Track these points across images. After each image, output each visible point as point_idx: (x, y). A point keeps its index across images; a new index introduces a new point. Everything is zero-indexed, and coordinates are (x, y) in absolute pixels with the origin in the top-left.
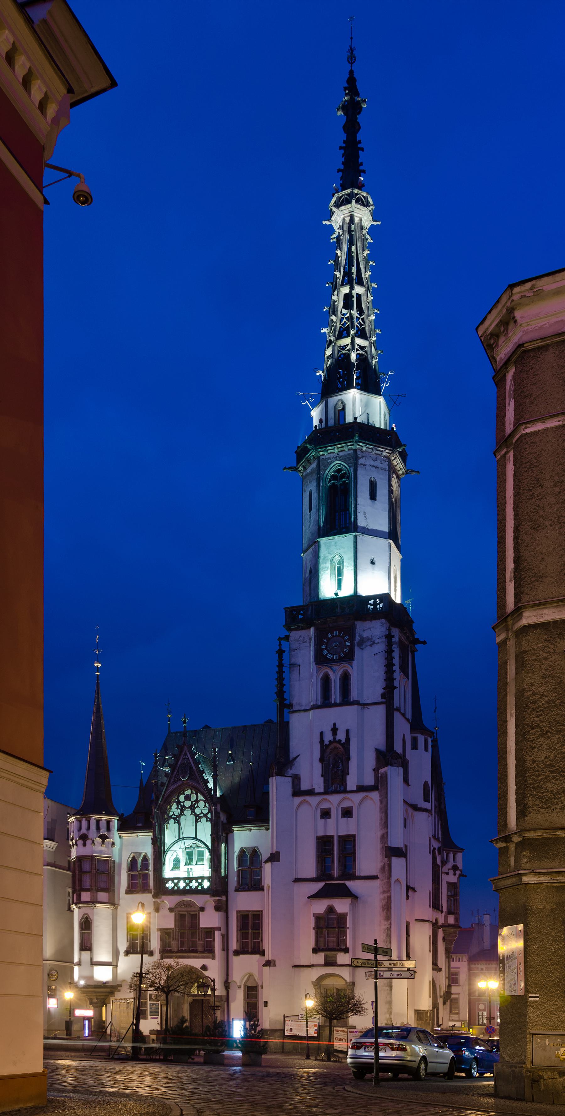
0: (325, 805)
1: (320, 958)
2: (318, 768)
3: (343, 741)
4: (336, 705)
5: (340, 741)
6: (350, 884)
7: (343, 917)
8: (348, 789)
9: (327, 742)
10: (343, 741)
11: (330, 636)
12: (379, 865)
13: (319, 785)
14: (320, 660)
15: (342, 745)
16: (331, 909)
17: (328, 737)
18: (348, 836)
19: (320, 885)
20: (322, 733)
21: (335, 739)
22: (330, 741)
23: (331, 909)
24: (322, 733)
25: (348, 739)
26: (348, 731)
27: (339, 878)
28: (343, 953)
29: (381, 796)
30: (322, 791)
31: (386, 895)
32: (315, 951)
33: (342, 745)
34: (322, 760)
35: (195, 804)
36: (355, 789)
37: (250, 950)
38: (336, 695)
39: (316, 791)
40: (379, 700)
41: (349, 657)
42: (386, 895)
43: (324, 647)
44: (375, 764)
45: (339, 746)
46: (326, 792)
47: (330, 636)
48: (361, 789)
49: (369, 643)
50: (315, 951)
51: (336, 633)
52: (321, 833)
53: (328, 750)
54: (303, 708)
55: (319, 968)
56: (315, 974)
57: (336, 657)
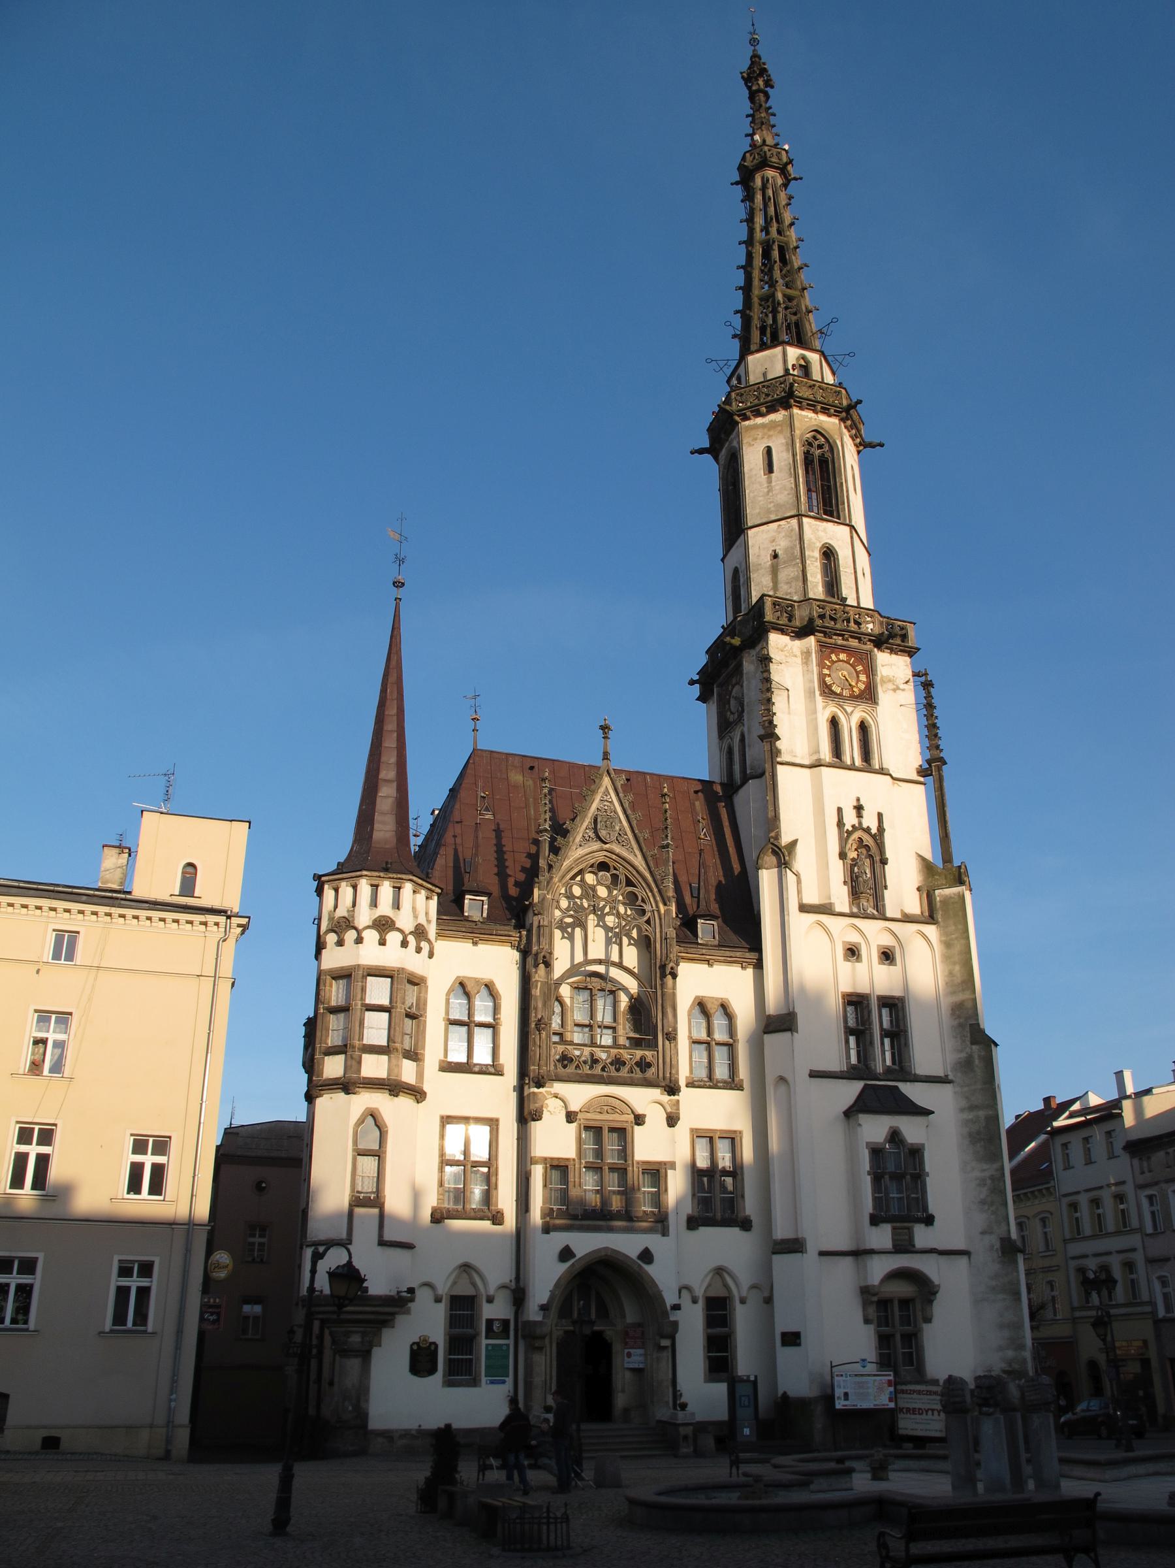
0: (854, 938)
1: (882, 1237)
2: (837, 871)
3: (874, 831)
4: (852, 768)
5: (867, 830)
6: (907, 1089)
7: (916, 1153)
8: (889, 913)
9: (848, 827)
10: (874, 831)
11: (834, 657)
12: (952, 1057)
13: (841, 898)
14: (827, 691)
15: (874, 837)
16: (895, 1136)
17: (850, 819)
18: (892, 998)
19: (856, 1087)
20: (840, 810)
21: (860, 823)
22: (853, 826)
23: (895, 1136)
24: (840, 810)
25: (881, 829)
26: (880, 816)
27: (889, 1073)
28: (923, 1226)
29: (944, 933)
30: (846, 910)
31: (982, 1114)
32: (875, 1221)
33: (874, 837)
34: (842, 855)
35: (575, 903)
36: (899, 916)
37: (719, 1216)
38: (852, 750)
39: (838, 909)
40: (914, 776)
41: (869, 695)
42: (982, 1114)
43: (826, 671)
44: (921, 878)
45: (866, 837)
46: (852, 915)
47: (834, 657)
48: (907, 919)
49: (891, 686)
50: (875, 1221)
51: (843, 656)
52: (849, 990)
53: (850, 841)
54: (798, 761)
55: (883, 1256)
56: (878, 1269)
57: (846, 693)
